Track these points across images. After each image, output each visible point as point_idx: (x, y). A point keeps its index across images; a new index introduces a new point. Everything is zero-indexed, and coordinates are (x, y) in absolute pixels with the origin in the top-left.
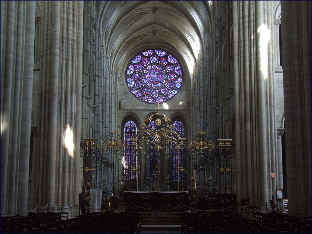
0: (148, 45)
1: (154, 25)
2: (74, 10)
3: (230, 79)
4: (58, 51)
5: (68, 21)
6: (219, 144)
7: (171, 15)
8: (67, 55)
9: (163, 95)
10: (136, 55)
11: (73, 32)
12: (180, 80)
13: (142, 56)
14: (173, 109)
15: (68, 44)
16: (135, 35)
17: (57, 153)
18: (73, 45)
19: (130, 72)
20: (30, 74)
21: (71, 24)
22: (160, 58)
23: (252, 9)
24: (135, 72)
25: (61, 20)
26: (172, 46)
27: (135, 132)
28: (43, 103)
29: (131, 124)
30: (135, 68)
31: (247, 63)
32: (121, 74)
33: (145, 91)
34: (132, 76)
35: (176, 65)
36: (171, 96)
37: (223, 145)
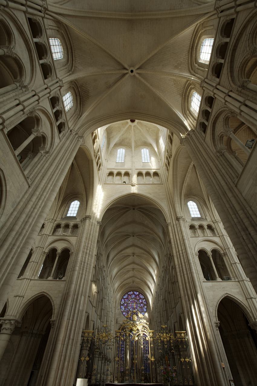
0: (131, 289)
1: (133, 278)
2: (90, 248)
3: (174, 295)
4: (77, 268)
5: (86, 253)
6: (176, 336)
7: (141, 272)
8: (83, 271)
11: (88, 259)
15: (84, 265)
16: (124, 283)
17: (62, 343)
19: (122, 303)
20: (28, 245)
21: (88, 255)
22: (136, 295)
23: (182, 247)
25: (82, 252)
26: (141, 289)
28: (62, 302)
30: (125, 301)
31: (186, 276)
32: (118, 304)
34: (123, 305)
35: (143, 299)
37: (180, 336)
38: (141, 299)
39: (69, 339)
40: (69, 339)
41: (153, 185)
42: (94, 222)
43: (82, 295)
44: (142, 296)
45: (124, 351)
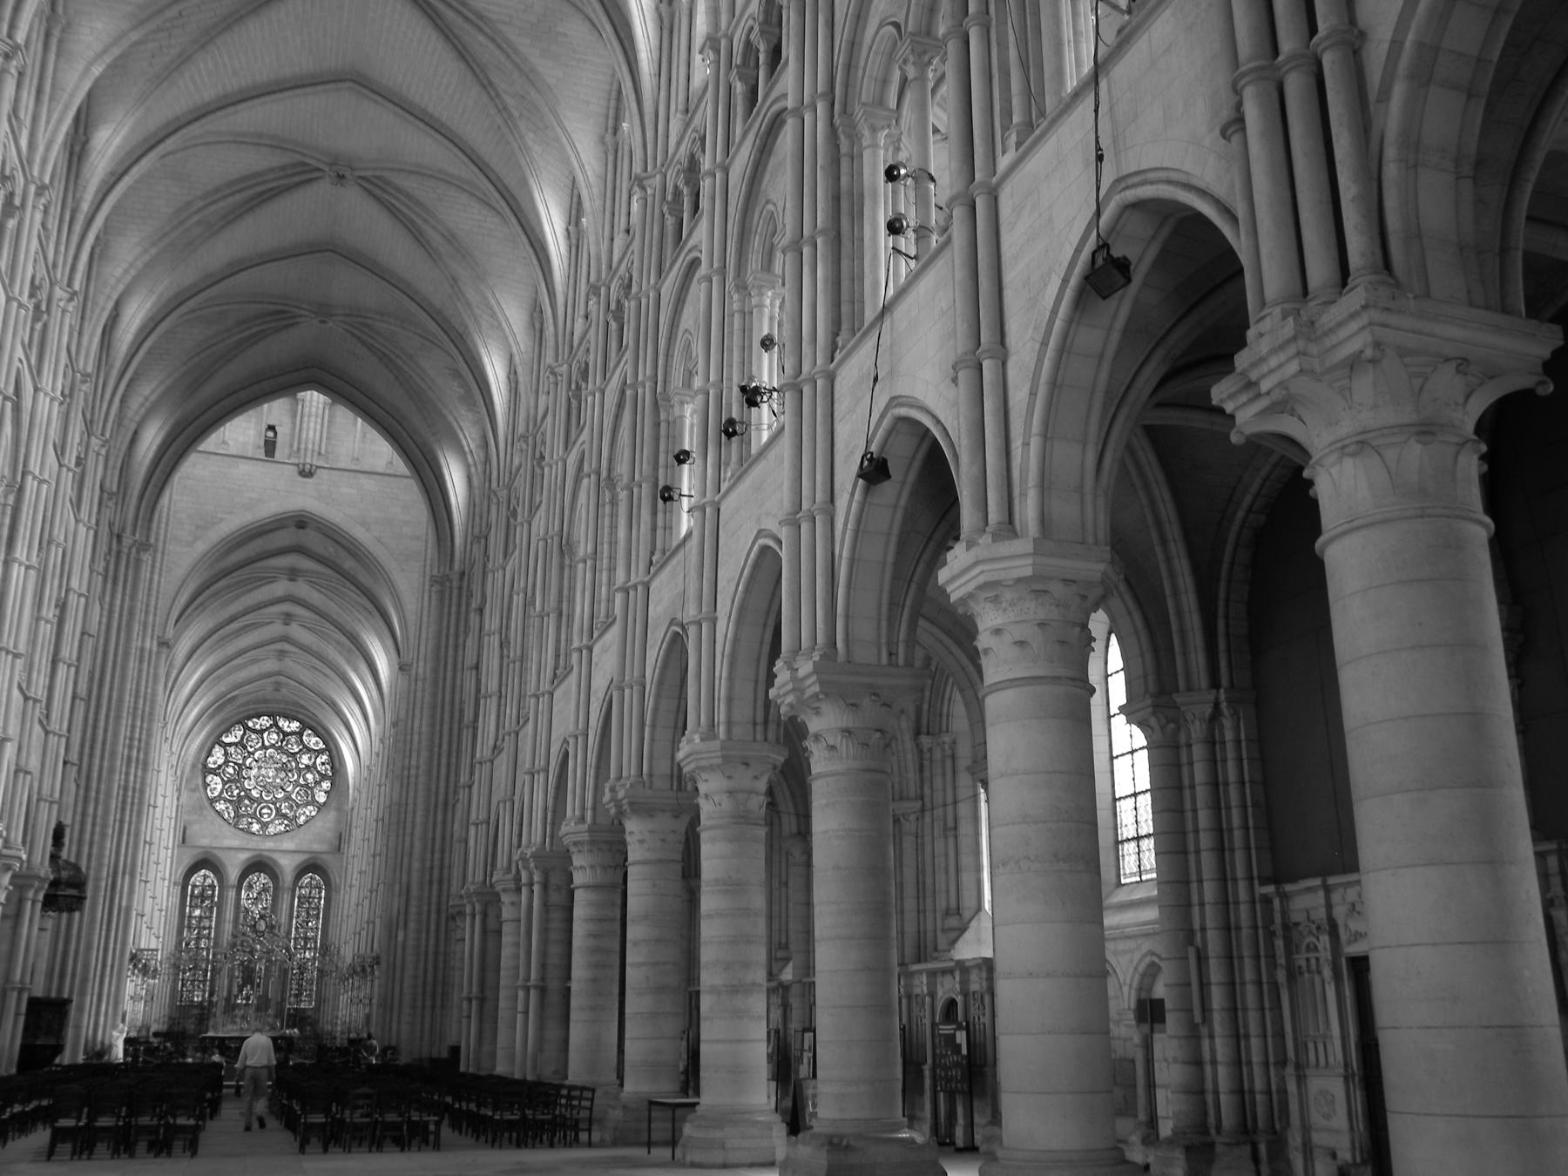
2: (140, 741)
9: (285, 816)
10: (233, 725)
11: (135, 776)
12: (326, 785)
13: (247, 728)
14: (305, 848)
15: (125, 796)
18: (133, 798)
21: (133, 765)
22: (286, 734)
24: (226, 763)
27: (213, 895)
29: (205, 877)
30: (226, 754)
31: (408, 838)
32: (194, 766)
33: (246, 806)
35: (319, 752)
36: (303, 818)
38: (309, 750)
39: (104, 965)
40: (104, 965)
41: (386, 478)
42: (148, 645)
43: (124, 873)
44: (314, 739)
45: (209, 938)
